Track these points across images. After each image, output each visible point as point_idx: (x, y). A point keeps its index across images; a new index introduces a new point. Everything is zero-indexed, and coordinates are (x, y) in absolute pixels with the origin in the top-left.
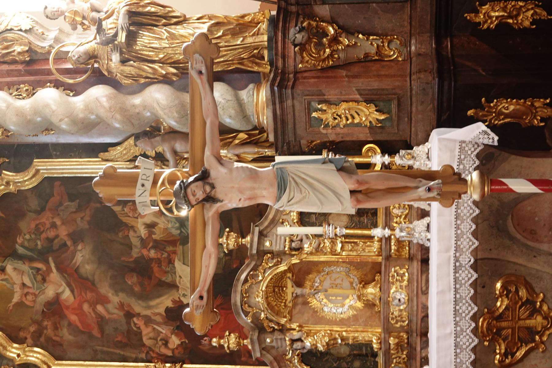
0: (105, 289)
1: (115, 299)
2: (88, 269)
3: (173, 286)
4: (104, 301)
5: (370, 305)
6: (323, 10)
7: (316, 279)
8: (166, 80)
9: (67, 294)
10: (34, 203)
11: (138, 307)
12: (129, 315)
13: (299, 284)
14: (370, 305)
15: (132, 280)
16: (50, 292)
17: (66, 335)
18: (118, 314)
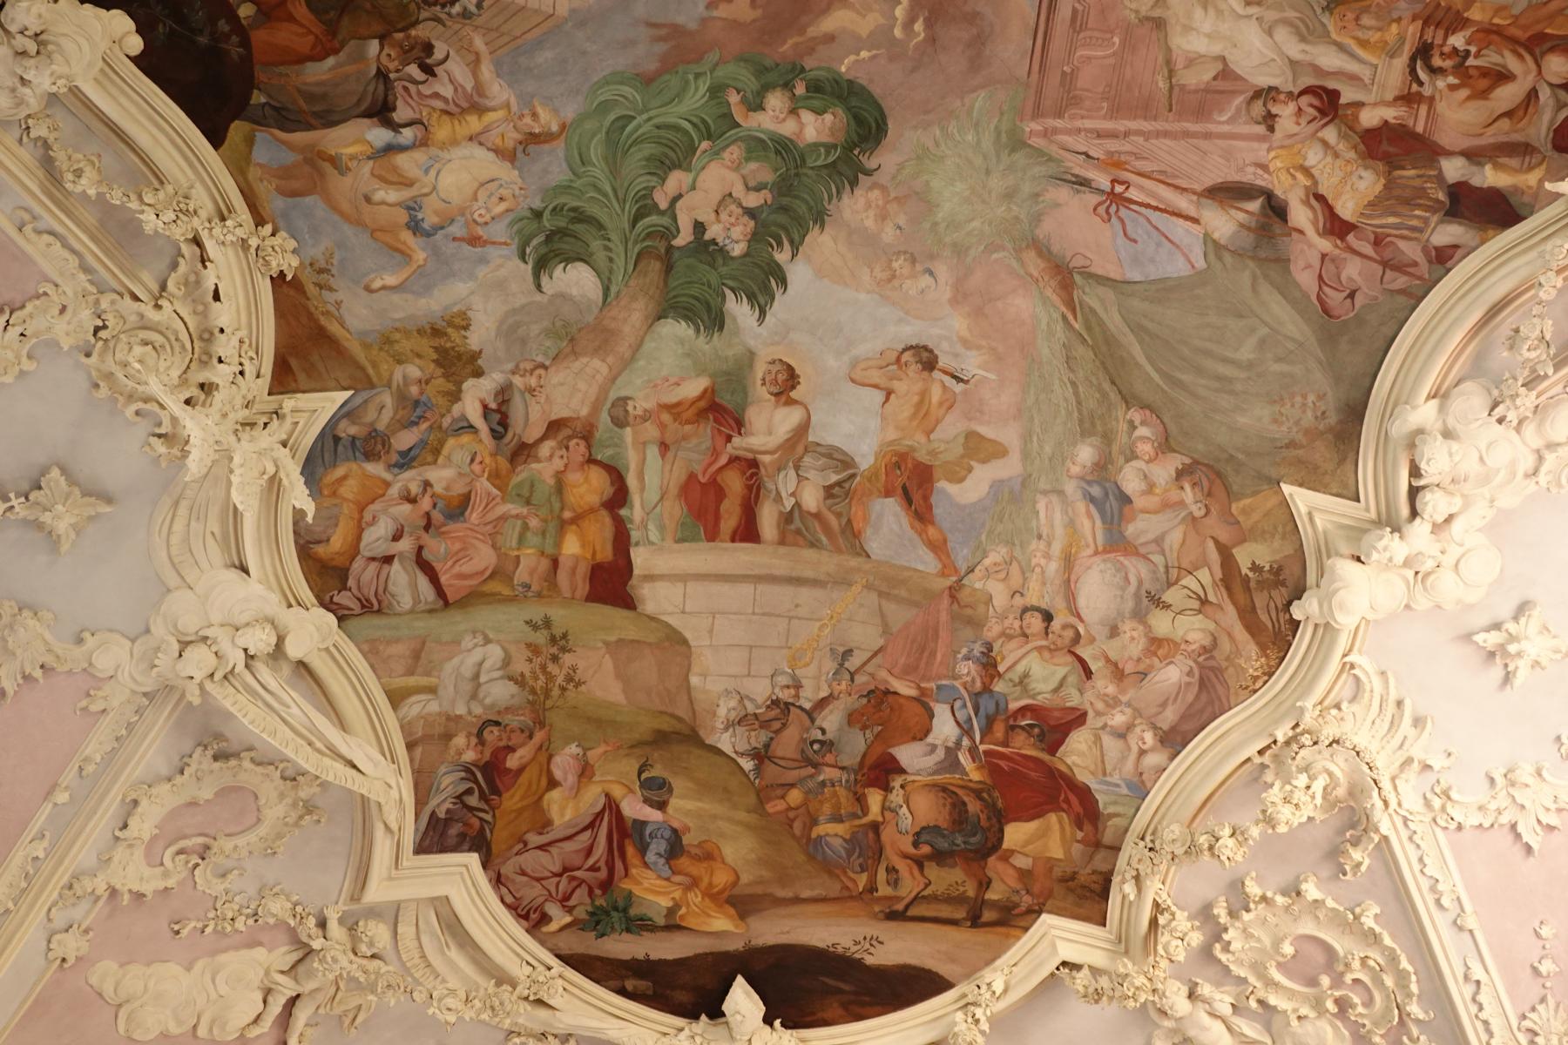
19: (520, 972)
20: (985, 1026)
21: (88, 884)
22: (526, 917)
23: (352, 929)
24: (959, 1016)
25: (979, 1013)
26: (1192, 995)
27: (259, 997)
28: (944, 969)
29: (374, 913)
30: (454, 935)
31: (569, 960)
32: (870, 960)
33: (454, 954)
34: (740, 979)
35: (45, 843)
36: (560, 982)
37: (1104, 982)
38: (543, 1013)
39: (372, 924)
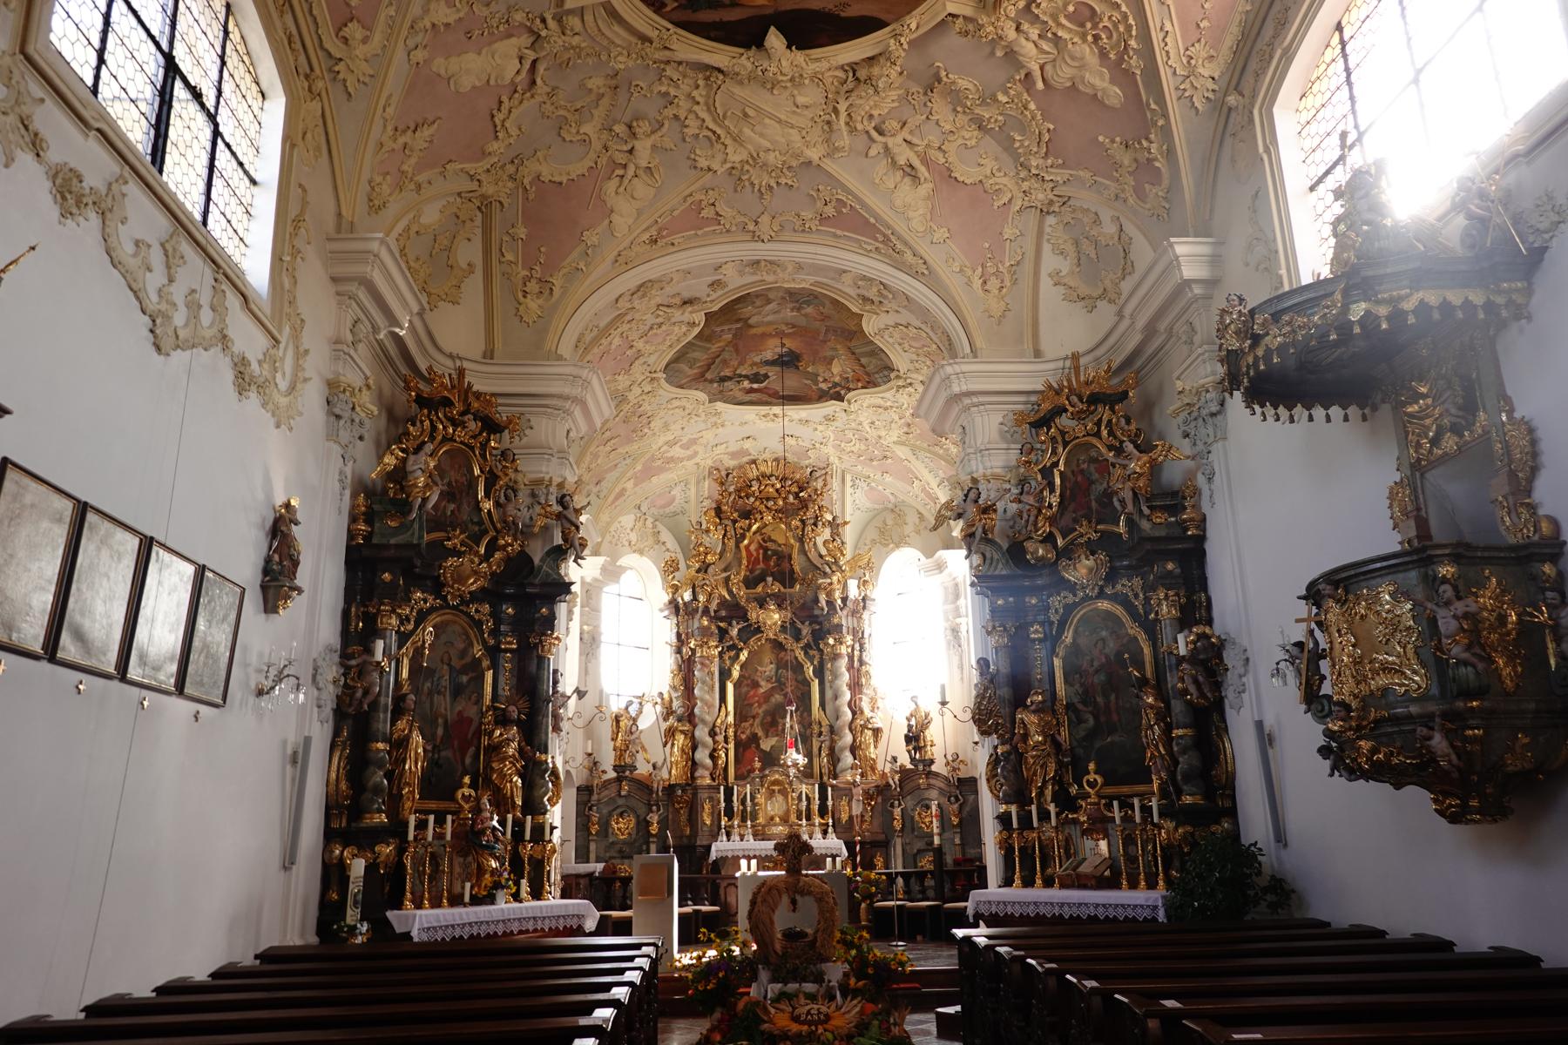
0: (764, 707)
1: (760, 711)
2: (773, 700)
3: (767, 737)
4: (760, 706)
5: (772, 818)
6: (880, 800)
7: (780, 798)
8: (854, 740)
9: (762, 690)
10: (800, 678)
11: (758, 721)
12: (754, 717)
13: (779, 791)
14: (772, 818)
15: (769, 719)
16: (763, 683)
17: (744, 689)
18: (754, 712)
19: (653, 34)
20: (906, 46)
21: (421, 25)
22: (653, 5)
23: (560, 21)
24: (892, 41)
25: (903, 40)
26: (1018, 29)
27: (517, 61)
28: (884, 17)
29: (571, 12)
30: (614, 18)
31: (678, 24)
32: (843, 14)
33: (617, 28)
34: (772, 29)
35: (394, 8)
36: (675, 37)
37: (971, 27)
38: (667, 53)
39: (570, 18)
